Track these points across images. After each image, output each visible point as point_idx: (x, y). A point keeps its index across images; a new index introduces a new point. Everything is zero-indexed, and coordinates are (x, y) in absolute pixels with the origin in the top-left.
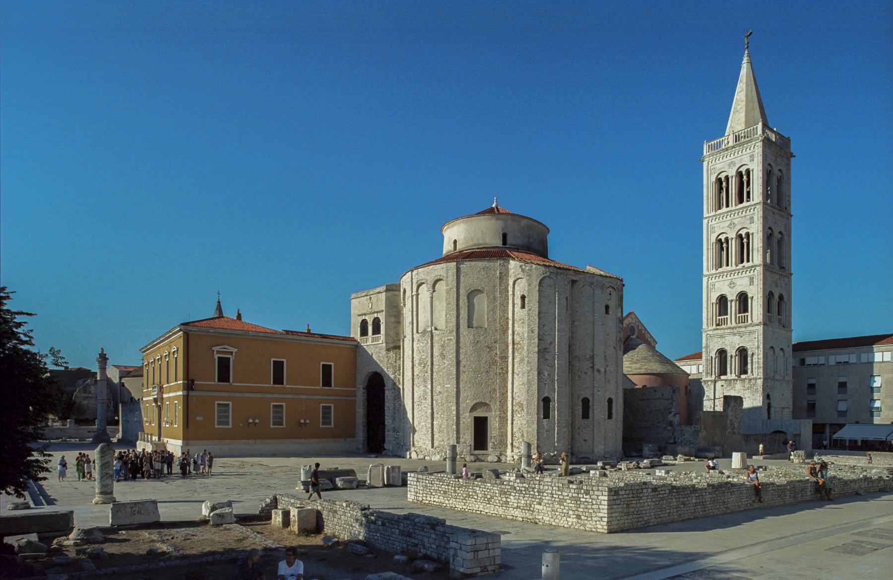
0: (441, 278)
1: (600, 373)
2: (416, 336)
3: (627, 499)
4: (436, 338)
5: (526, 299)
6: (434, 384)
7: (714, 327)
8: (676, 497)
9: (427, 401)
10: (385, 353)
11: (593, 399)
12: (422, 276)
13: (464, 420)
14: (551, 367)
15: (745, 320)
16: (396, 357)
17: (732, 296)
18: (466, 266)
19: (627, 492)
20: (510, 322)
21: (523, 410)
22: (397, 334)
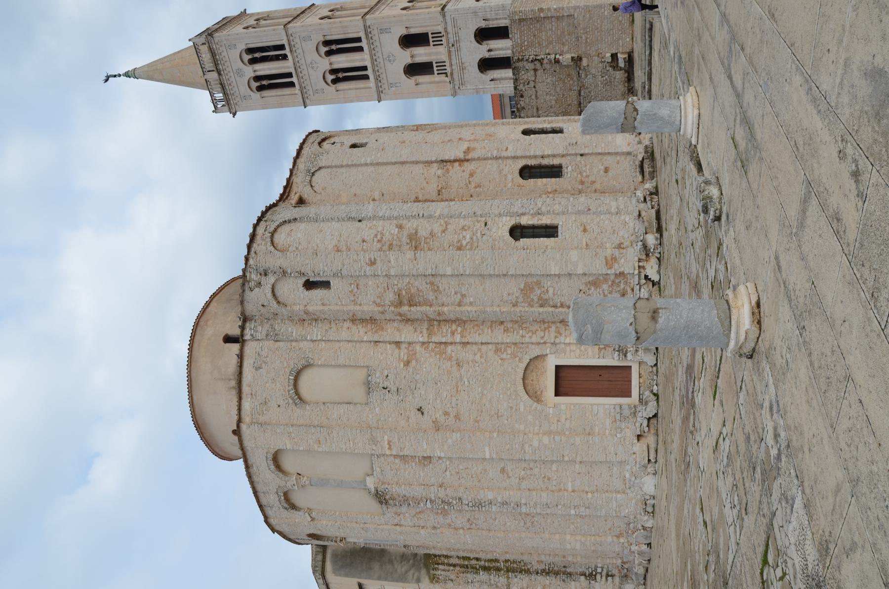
1: (474, 149)
7: (447, 79)
9: (523, 501)
10: (437, 585)
11: (522, 157)
12: (272, 499)
14: (447, 224)
16: (443, 564)
17: (406, 57)
22: (403, 557)
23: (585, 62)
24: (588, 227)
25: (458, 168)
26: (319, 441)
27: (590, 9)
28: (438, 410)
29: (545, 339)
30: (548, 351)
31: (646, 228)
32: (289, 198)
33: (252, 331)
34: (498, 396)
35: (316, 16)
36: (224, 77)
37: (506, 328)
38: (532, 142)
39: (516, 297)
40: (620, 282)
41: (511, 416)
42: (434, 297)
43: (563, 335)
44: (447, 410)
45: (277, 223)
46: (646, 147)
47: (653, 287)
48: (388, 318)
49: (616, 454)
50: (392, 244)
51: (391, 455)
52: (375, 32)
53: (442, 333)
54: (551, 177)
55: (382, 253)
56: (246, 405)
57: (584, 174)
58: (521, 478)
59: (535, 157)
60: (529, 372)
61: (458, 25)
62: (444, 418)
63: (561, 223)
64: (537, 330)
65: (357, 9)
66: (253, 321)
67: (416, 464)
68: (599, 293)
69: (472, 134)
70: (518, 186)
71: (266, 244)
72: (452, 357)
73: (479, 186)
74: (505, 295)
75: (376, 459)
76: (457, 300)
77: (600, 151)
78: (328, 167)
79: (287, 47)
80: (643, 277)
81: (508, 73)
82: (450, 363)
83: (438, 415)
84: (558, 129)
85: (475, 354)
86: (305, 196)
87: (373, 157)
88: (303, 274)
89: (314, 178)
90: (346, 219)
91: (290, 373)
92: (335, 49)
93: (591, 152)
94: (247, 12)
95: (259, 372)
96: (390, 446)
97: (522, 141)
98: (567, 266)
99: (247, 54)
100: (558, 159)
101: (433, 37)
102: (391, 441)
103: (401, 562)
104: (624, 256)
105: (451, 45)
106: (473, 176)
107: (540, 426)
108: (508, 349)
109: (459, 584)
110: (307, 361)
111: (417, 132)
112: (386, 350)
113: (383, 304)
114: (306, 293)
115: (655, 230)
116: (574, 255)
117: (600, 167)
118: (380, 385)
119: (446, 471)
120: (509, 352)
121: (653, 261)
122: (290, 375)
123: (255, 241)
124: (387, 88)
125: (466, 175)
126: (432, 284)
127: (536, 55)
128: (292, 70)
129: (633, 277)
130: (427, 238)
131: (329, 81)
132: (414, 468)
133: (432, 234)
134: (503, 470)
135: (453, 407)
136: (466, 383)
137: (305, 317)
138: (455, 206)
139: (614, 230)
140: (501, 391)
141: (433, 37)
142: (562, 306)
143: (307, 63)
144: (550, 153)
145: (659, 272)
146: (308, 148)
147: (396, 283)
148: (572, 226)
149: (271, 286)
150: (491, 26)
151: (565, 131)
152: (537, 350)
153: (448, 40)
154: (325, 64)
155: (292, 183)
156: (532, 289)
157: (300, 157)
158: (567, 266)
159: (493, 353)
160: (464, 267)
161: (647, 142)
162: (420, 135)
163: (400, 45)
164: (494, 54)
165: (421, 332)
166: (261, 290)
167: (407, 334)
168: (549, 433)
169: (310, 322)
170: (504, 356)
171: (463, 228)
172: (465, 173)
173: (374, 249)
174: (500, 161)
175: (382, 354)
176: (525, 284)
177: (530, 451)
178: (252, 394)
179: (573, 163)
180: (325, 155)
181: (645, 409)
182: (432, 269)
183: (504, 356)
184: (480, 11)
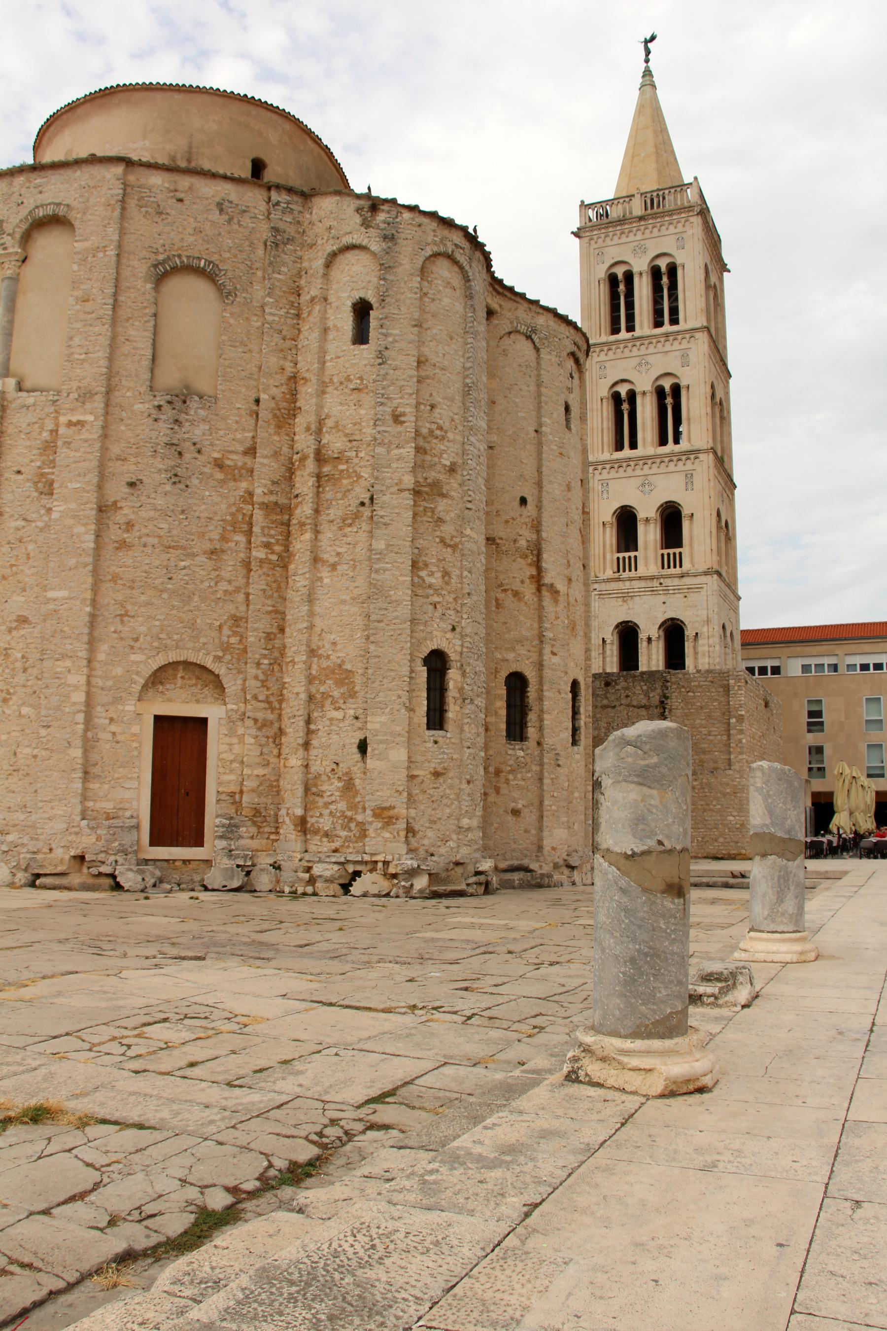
0: (62, 211)
7: (609, 573)
11: (541, 678)
13: (113, 728)
14: (454, 547)
15: (678, 561)
21: (352, 694)
24: (441, 780)
25: (528, 574)
26: (87, 300)
27: (738, 795)
28: (137, 513)
29: (253, 702)
30: (230, 706)
31: (437, 874)
32: (494, 293)
33: (285, 206)
34: (159, 617)
35: (716, 378)
36: (634, 225)
37: (272, 636)
38: (563, 695)
39: (328, 657)
40: (350, 830)
41: (122, 639)
42: (331, 517)
43: (258, 733)
44: (136, 528)
46: (550, 876)
47: (340, 885)
48: (296, 438)
49: (49, 819)
50: (426, 453)
51: (57, 425)
52: (689, 466)
53: (269, 528)
54: (509, 723)
55: (413, 435)
56: (157, 180)
57: (511, 777)
58: (9, 652)
59: (540, 699)
60: (197, 671)
61: (692, 594)
62: (122, 521)
63: (449, 735)
64: (268, 689)
65: (722, 442)
66: (301, 209)
67: (39, 467)
68: (331, 795)
69: (576, 601)
70: (496, 668)
71: (435, 243)
72: (227, 543)
73: (498, 606)
74: (332, 637)
75: (51, 398)
76: (325, 556)
77: (546, 803)
78: (538, 363)
79: (675, 328)
80: (359, 868)
81: (612, 666)
82: (217, 537)
83: (126, 511)
84: (577, 738)
85: (230, 582)
87: (550, 437)
88: (383, 300)
89: (522, 339)
90: (468, 381)
91: (212, 262)
92: (667, 401)
93: (545, 788)
94: (725, 274)
95: (214, 208)
96: (76, 424)
97: (565, 679)
98: (381, 742)
99: (668, 265)
100: (535, 735)
101: (674, 554)
102: (83, 426)
104: (394, 837)
105: (662, 581)
106: (514, 596)
107: (102, 689)
108: (238, 638)
110: (229, 294)
111: (580, 511)
112: (244, 430)
113: (324, 430)
114: (349, 303)
115: (435, 888)
116: (400, 755)
117: (520, 801)
118: (183, 415)
119: (24, 519)
120: (233, 640)
121: (384, 885)
122: (206, 260)
123: (440, 226)
124: (600, 477)
125: (516, 586)
126: (357, 516)
127: (670, 710)
128: (638, 333)
129: (358, 852)
130: (433, 512)
131: (617, 388)
132: (33, 464)
134: (23, 620)
135: (140, 538)
136: (182, 564)
137: (305, 298)
138: (481, 562)
139: (435, 822)
140: (166, 623)
141: (674, 554)
142: (309, 732)
143: (648, 357)
144: (545, 722)
145: (365, 895)
146: (568, 334)
147: (360, 455)
148: (444, 753)
149: (364, 244)
150: (686, 644)
151: (576, 748)
152: (233, 688)
153: (670, 577)
154: (644, 384)
155: (517, 302)
156: (339, 683)
157: (556, 319)
158: (381, 742)
159: (232, 612)
160: (385, 570)
161: (556, 877)
162: (577, 516)
163: (666, 503)
164: (643, 646)
165: (271, 492)
166: (357, 227)
168: (89, 703)
169: (296, 305)
170: (226, 631)
172: (519, 583)
173: (420, 423)
174: (536, 642)
175: (237, 422)
176: (350, 671)
177: (58, 670)
178: (176, 191)
179: (529, 760)
180: (557, 359)
181: (131, 870)
182: (382, 517)
183: (226, 631)
184: (711, 630)
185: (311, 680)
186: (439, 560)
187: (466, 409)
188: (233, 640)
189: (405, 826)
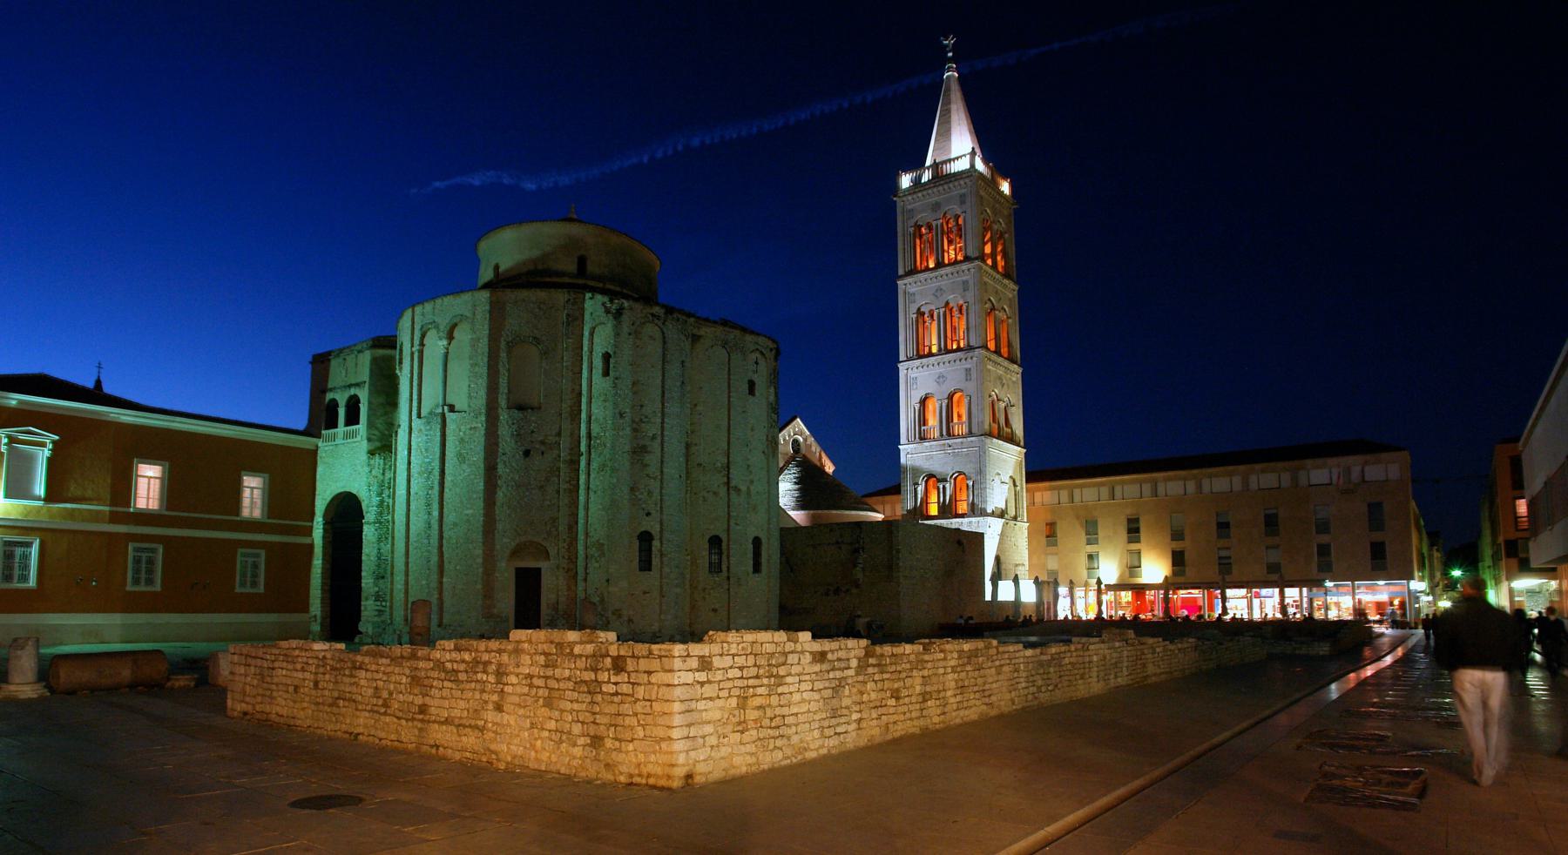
1: (739, 495)
2: (416, 423)
3: (739, 683)
4: (451, 427)
5: (612, 361)
6: (445, 510)
8: (877, 677)
14: (655, 478)
16: (385, 464)
18: (511, 295)
19: (740, 661)
20: (584, 400)
21: (603, 554)
23: (854, 591)
24: (647, 595)
45: (662, 327)
57: (712, 591)
63: (651, 573)
73: (705, 500)
82: (543, 479)
85: (551, 502)
86: (702, 340)
103: (386, 423)
109: (367, 478)
133: (646, 465)
142: (587, 573)
147: (607, 434)
167: (565, 442)
171: (650, 493)
185: (586, 548)
186: (646, 486)
187: (663, 404)
188: (553, 529)
189: (626, 619)
